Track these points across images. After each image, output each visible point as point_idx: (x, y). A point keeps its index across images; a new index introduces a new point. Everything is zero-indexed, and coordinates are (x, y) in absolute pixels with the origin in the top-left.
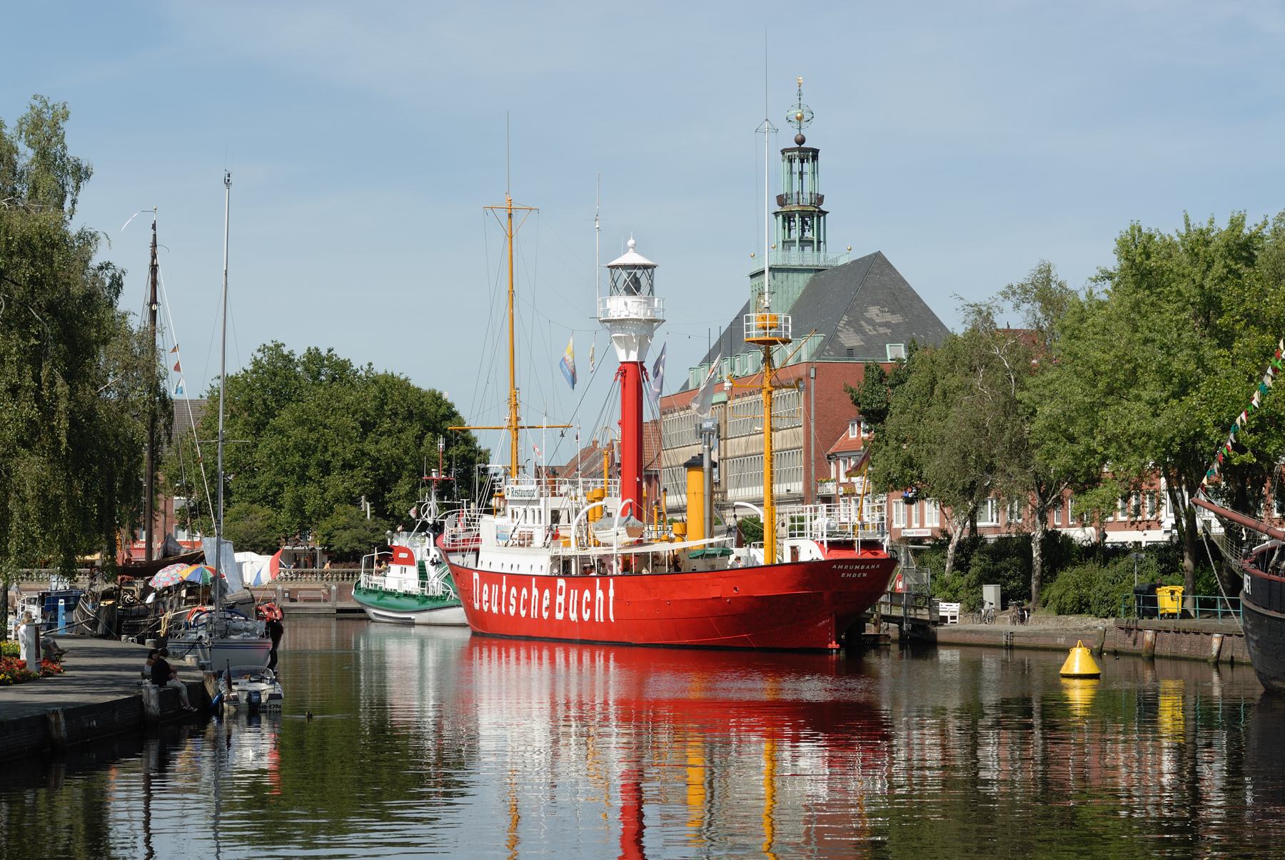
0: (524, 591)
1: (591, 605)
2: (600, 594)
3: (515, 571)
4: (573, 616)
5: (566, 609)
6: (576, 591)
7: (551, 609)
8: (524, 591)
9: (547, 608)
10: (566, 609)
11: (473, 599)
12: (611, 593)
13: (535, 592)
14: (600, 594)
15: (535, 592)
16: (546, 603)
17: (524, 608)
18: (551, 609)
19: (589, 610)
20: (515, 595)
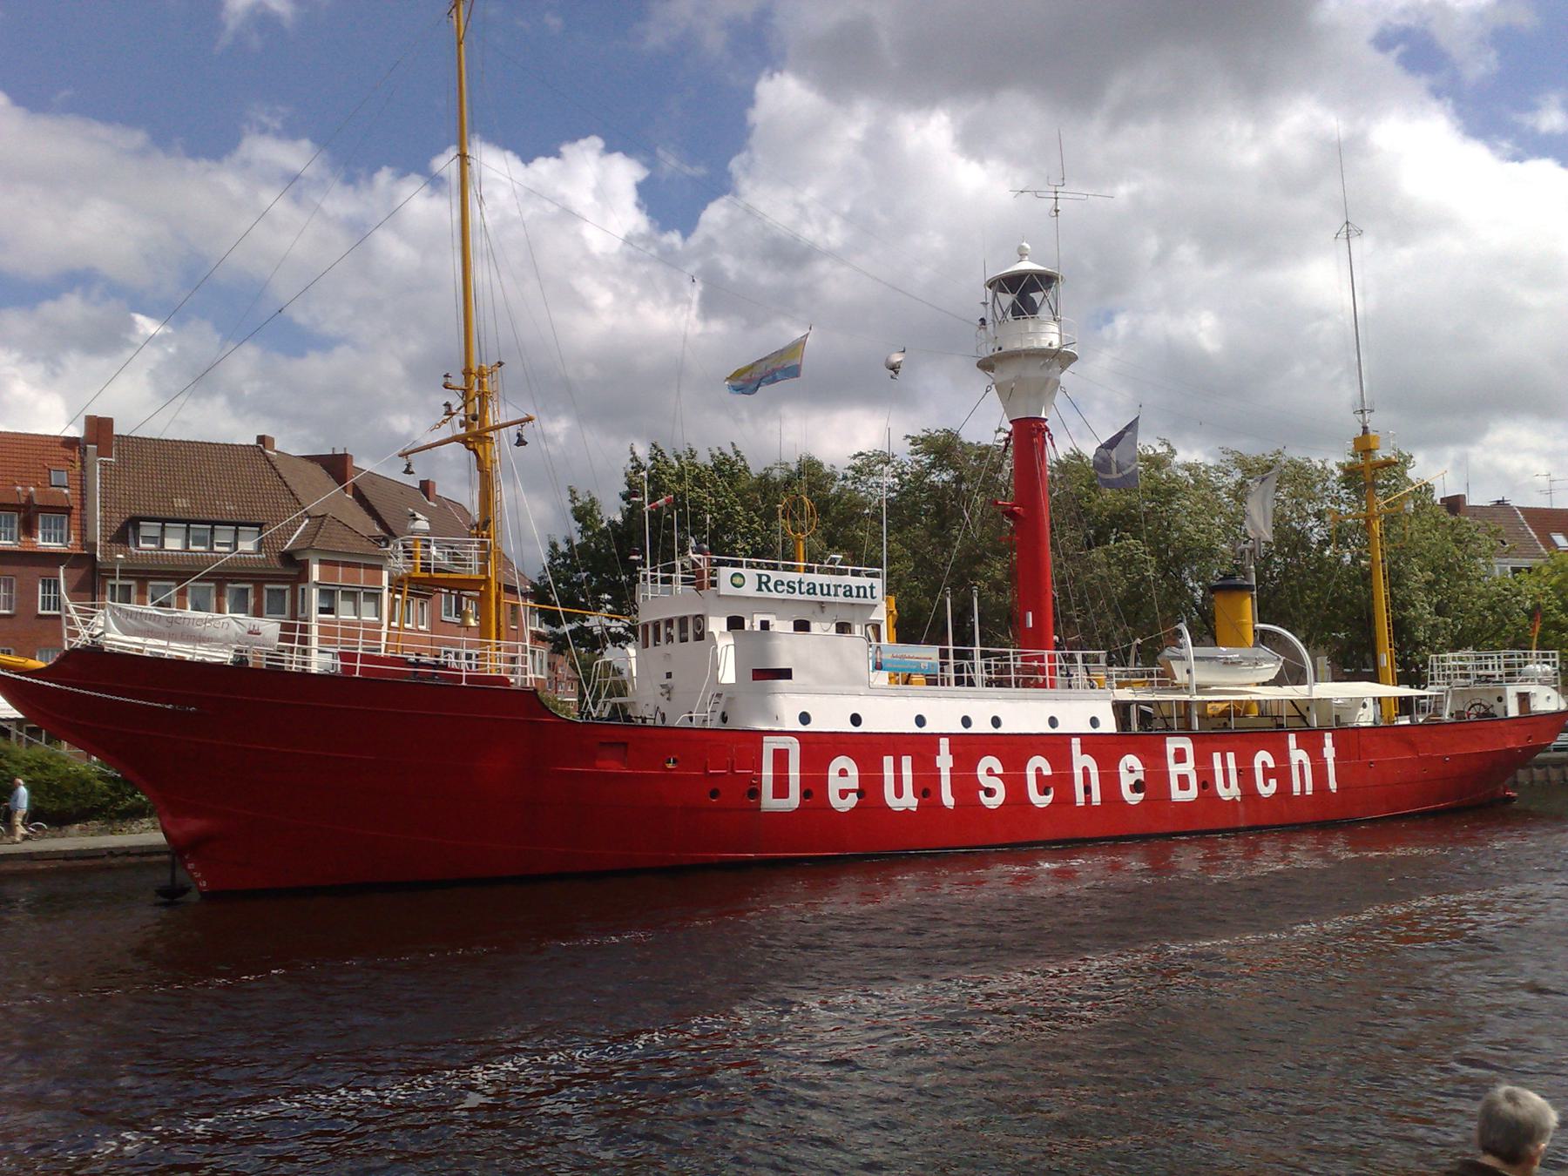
0: (1038, 764)
1: (1281, 772)
2: (1298, 755)
3: (982, 726)
4: (1229, 791)
5: (1206, 783)
6: (1231, 756)
7: (1154, 783)
8: (1038, 764)
9: (1137, 787)
10: (1206, 783)
11: (756, 793)
12: (1329, 752)
13: (1082, 762)
14: (1298, 755)
15: (1082, 762)
16: (1126, 781)
17: (1043, 791)
18: (1154, 783)
19: (1273, 782)
20: (999, 770)
